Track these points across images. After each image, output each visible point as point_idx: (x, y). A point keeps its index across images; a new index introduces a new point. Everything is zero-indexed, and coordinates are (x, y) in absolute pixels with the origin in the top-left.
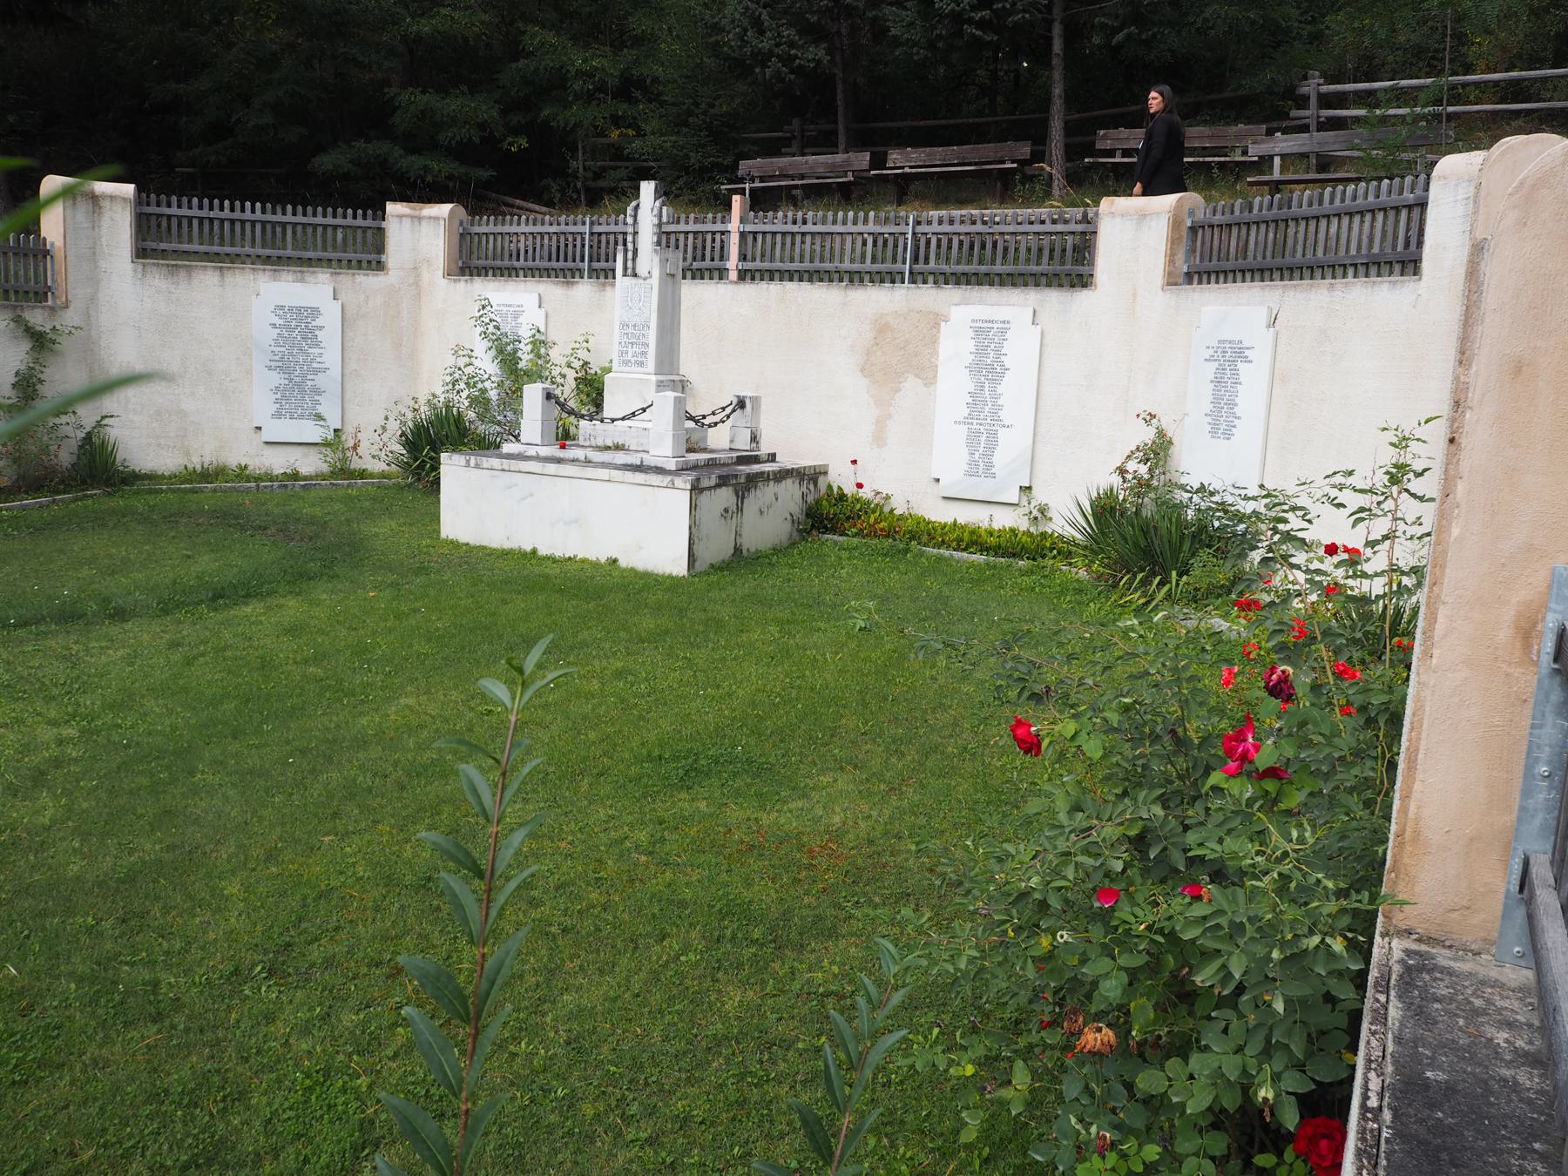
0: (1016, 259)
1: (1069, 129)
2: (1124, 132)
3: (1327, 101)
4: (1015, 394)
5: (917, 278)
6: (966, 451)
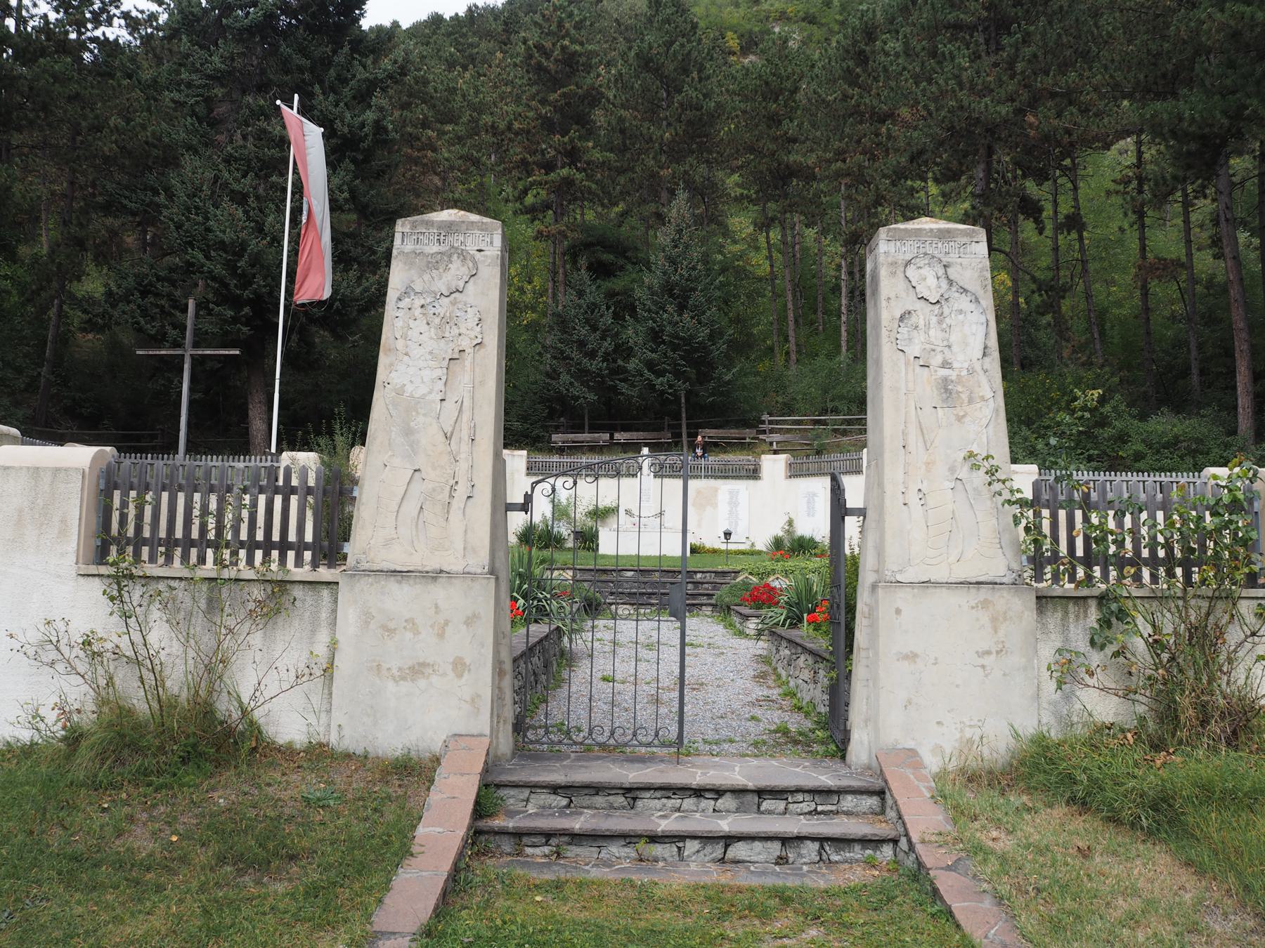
1: (688, 426)
3: (771, 422)
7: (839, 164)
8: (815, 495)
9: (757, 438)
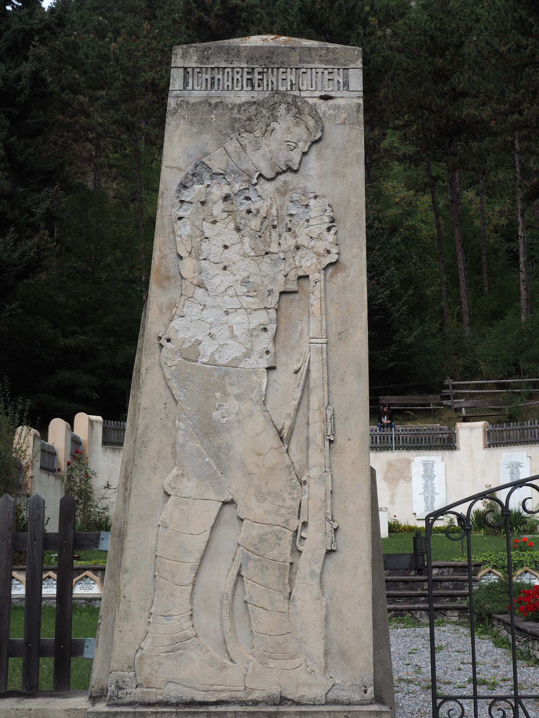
0: (429, 442)
2: (389, 397)
3: (455, 387)
4: (439, 483)
5: (398, 448)
7: (516, 116)
8: (519, 465)
9: (441, 404)
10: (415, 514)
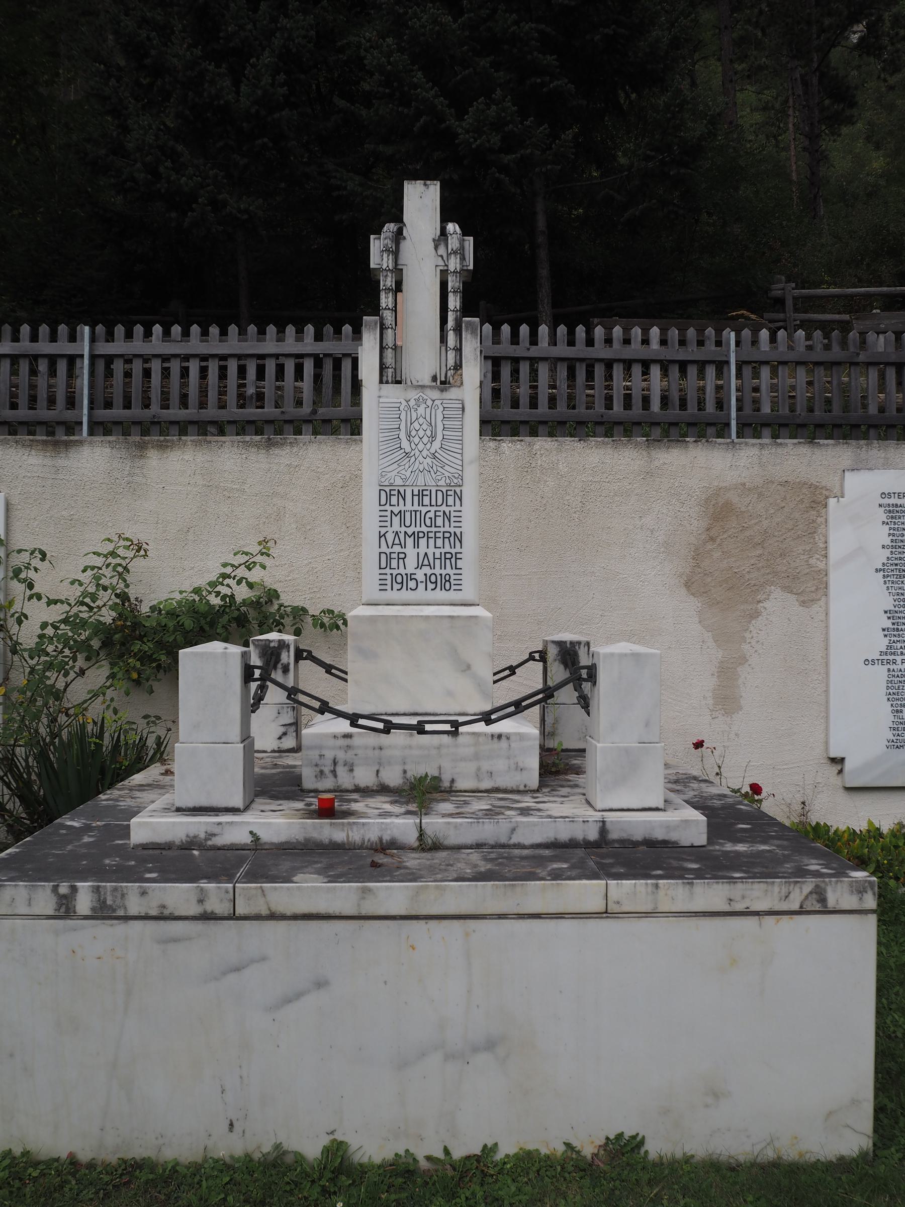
6: (887, 708)
10: (838, 761)
